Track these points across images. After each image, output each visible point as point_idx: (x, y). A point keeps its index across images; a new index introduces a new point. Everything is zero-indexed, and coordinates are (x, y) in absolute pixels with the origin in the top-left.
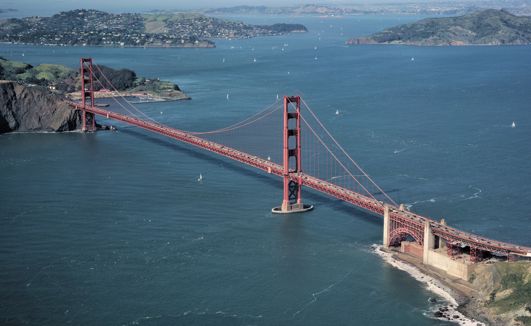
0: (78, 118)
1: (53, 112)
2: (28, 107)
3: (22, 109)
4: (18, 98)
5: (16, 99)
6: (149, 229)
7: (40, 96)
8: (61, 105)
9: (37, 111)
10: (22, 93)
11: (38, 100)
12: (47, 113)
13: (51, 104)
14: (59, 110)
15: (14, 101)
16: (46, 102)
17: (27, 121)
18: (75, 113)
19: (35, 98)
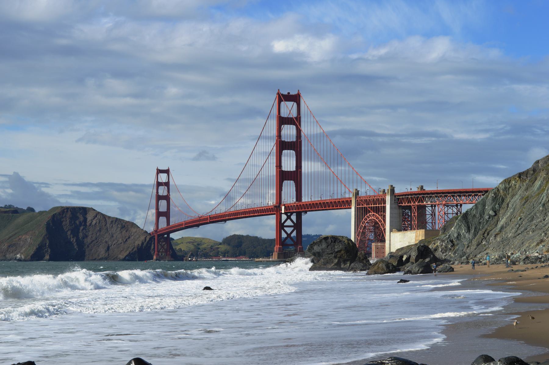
0: (153, 246)
1: (125, 240)
2: (98, 235)
3: (90, 237)
4: (88, 224)
7: (114, 222)
8: (136, 232)
9: (107, 239)
10: (94, 219)
11: (111, 226)
14: (132, 237)
15: (82, 228)
16: (119, 229)
17: (93, 251)
18: (149, 241)
19: (108, 225)
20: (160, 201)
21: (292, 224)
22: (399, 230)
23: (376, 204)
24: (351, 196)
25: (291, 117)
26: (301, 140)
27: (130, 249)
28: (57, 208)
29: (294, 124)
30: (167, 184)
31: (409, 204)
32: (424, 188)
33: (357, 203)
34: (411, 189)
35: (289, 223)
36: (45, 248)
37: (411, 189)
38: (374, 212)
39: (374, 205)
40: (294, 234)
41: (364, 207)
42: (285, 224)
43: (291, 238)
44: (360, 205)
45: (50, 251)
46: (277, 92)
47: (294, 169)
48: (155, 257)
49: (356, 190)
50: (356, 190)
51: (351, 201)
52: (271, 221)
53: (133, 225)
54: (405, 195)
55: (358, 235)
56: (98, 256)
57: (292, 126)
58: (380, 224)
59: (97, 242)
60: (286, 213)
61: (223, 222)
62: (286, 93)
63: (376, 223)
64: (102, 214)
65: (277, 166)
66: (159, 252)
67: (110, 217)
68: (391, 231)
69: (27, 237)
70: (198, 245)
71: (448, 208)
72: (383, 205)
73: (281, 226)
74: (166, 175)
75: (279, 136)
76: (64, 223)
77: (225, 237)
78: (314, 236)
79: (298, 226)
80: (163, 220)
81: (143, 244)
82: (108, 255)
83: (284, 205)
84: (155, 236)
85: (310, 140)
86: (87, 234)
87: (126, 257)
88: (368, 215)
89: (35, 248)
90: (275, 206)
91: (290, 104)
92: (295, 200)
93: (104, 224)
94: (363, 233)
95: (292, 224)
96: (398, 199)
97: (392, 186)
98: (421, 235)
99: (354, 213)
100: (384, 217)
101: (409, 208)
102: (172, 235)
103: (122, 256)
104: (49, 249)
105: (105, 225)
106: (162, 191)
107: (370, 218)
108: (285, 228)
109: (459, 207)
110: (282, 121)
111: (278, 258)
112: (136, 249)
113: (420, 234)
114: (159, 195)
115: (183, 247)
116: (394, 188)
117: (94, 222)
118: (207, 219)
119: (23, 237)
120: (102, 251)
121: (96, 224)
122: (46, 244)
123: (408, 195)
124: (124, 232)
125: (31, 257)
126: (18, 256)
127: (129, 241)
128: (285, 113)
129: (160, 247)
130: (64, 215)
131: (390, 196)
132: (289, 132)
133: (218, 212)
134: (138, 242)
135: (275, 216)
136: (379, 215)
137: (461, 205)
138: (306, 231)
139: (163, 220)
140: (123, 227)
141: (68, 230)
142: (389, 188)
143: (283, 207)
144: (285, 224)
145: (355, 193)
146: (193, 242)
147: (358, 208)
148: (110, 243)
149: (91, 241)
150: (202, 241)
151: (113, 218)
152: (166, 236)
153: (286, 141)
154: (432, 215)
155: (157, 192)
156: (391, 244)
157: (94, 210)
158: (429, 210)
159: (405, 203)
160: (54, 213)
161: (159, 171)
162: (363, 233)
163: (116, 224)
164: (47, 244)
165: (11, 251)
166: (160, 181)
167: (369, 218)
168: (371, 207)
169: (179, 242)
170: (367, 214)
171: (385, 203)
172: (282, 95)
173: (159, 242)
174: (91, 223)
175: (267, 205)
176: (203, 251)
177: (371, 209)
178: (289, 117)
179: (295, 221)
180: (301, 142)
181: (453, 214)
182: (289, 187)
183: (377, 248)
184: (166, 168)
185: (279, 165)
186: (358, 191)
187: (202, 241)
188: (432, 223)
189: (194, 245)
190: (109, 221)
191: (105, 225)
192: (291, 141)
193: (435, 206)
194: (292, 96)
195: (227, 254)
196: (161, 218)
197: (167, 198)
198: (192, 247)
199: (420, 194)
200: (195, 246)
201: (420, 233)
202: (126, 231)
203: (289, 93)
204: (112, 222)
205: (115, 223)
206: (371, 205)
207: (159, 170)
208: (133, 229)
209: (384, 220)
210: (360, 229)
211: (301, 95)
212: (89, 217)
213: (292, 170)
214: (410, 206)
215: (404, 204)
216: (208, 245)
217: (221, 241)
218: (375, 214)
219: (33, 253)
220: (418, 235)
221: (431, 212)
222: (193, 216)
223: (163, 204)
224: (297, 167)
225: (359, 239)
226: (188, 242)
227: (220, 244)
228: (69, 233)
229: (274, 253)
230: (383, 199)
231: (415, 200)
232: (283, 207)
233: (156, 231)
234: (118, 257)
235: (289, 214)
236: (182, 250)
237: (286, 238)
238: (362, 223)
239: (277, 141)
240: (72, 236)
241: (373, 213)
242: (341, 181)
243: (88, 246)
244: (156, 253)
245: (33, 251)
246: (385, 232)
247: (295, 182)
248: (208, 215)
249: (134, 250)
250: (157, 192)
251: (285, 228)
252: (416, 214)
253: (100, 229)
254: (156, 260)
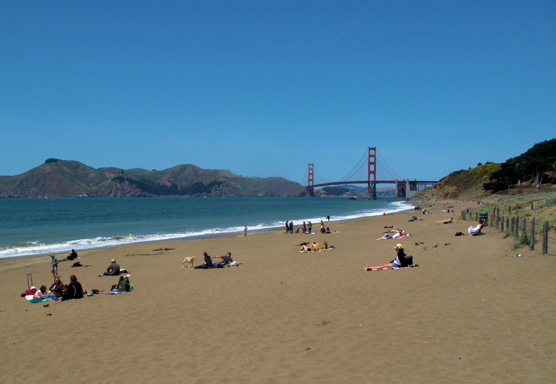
30: (312, 169)
73: (369, 187)
75: (369, 161)
79: (374, 187)
80: (311, 182)
91: (372, 150)
106: (311, 172)
152: (312, 188)
161: (309, 165)
185: (369, 169)
194: (373, 148)
196: (310, 182)
197: (312, 174)
224: (374, 170)
227: (321, 190)
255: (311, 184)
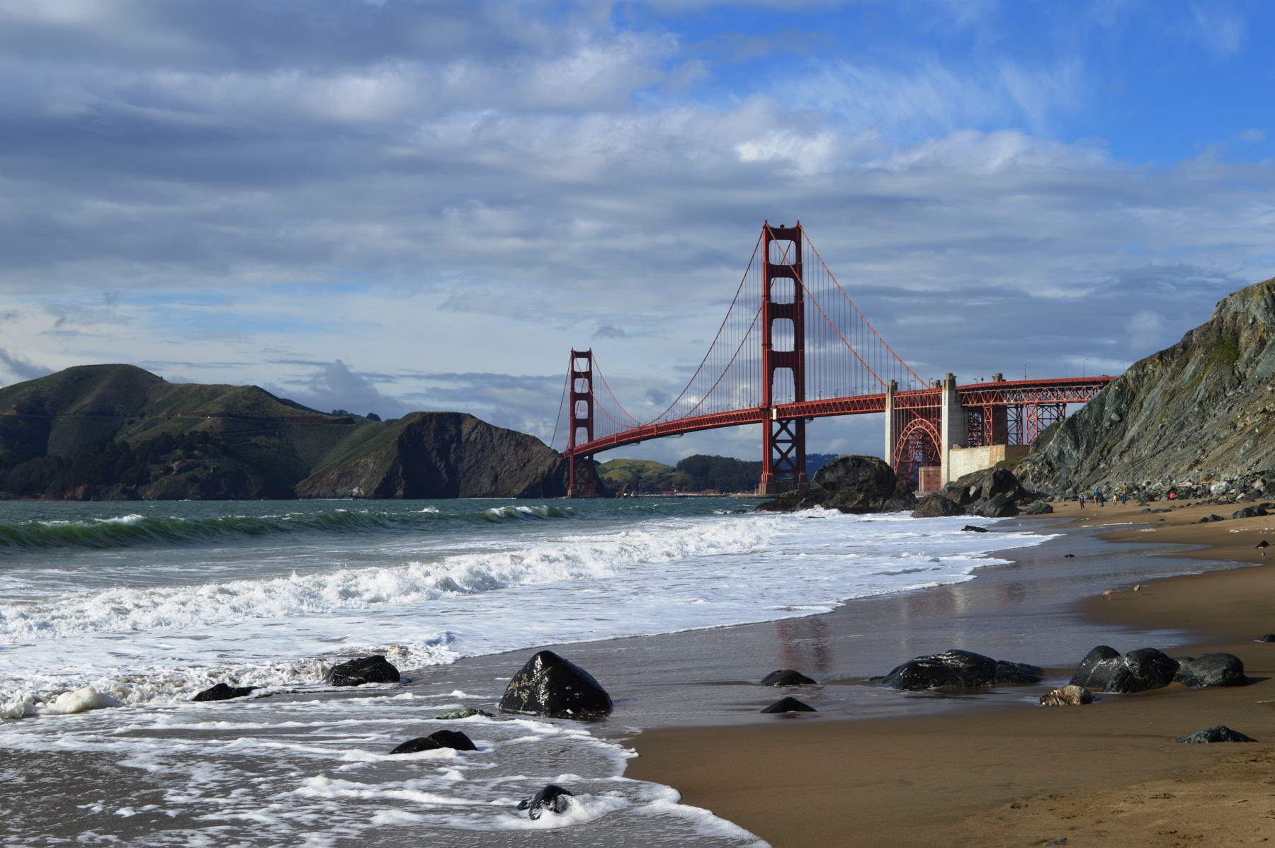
0: (566, 473)
1: (522, 465)
2: (479, 456)
3: (467, 459)
4: (463, 440)
5: (459, 441)
6: (677, 701)
7: (505, 436)
8: (539, 452)
9: (494, 464)
10: (473, 431)
11: (499, 443)
12: (511, 466)
13: (521, 451)
14: (534, 460)
15: (454, 446)
16: (513, 447)
17: (472, 481)
18: (561, 465)
19: (495, 441)
20: (577, 402)
21: (791, 439)
22: (964, 446)
23: (926, 405)
24: (885, 391)
25: (787, 264)
26: (803, 303)
27: (530, 480)
28: (415, 414)
29: (792, 276)
30: (588, 375)
31: (980, 404)
32: (1003, 378)
33: (895, 403)
34: (982, 380)
35: (784, 435)
36: (398, 478)
37: (982, 380)
38: (922, 417)
39: (922, 405)
40: (793, 454)
41: (907, 410)
42: (778, 438)
43: (789, 461)
44: (899, 406)
45: (404, 483)
46: (763, 225)
47: (792, 349)
48: (570, 492)
49: (893, 381)
50: (893, 381)
51: (884, 399)
52: (755, 431)
53: (535, 440)
54: (974, 389)
55: (896, 455)
56: (480, 490)
57: (787, 279)
58: (932, 437)
59: (478, 469)
60: (778, 420)
61: (677, 435)
62: (778, 226)
63: (926, 435)
64: (485, 423)
65: (764, 345)
66: (575, 482)
67: (498, 428)
68: (950, 447)
69: (369, 461)
70: (639, 471)
71: (1044, 410)
72: (936, 406)
73: (771, 441)
74: (585, 360)
75: (767, 295)
76: (425, 438)
77: (682, 459)
78: (825, 456)
79: (799, 440)
80: (582, 433)
81: (550, 470)
82: (496, 489)
83: (776, 407)
84: (569, 458)
85: (817, 302)
86: (462, 455)
87: (524, 492)
88: (913, 421)
89: (381, 478)
90: (762, 409)
91: (786, 242)
92: (794, 400)
93: (488, 439)
94: (905, 451)
95: (791, 439)
96: (961, 397)
97: (951, 375)
98: (998, 454)
99: (890, 418)
100: (939, 425)
101: (980, 410)
102: (596, 457)
103: (517, 491)
104: (403, 480)
105: (491, 442)
106: (581, 385)
107: (916, 427)
108: (778, 445)
109: (1061, 408)
110: (772, 271)
111: (767, 493)
112: (540, 478)
113: (997, 452)
114: (575, 393)
115: (615, 476)
116: (954, 378)
117: (473, 436)
118: (652, 430)
119: (362, 461)
120: (486, 482)
121: (476, 439)
122: (398, 471)
123: (978, 389)
124: (521, 451)
125: (376, 492)
126: (355, 490)
127: (529, 467)
128: (776, 259)
129: (577, 476)
130: (426, 426)
131: (949, 390)
132: (783, 290)
133: (670, 419)
134: (543, 468)
135: (762, 424)
136: (930, 422)
137: (1064, 405)
138: (810, 449)
139: (582, 433)
140: (519, 444)
141: (433, 449)
142: (946, 378)
143: (775, 411)
144: (778, 438)
145: (892, 386)
146: (630, 468)
147: (896, 410)
148: (498, 469)
149: (468, 466)
150: (644, 465)
151: (503, 429)
152: (587, 458)
153: (778, 303)
154: (1016, 421)
155: (573, 388)
156: (950, 468)
157: (473, 417)
158: (1011, 414)
159: (973, 403)
160: (411, 422)
161: (576, 355)
162: (905, 451)
163: (508, 439)
164: (400, 472)
165: (344, 483)
166: (576, 369)
167: (914, 427)
168: (918, 409)
169: (608, 467)
170: (911, 421)
171: (939, 402)
172: (772, 229)
173: (575, 467)
174: (469, 438)
175: (749, 408)
176: (646, 481)
177: (918, 413)
178: (783, 264)
179: (794, 433)
180: (802, 305)
181: (1051, 419)
182: (784, 377)
183: (927, 475)
184: (586, 350)
185: (768, 343)
186: (896, 384)
187: (644, 465)
188: (1017, 434)
189: (631, 472)
190: (496, 436)
191: (491, 442)
192: (786, 303)
193: (1022, 407)
194: (788, 230)
195: (684, 487)
197: (588, 397)
198: (629, 475)
199: (997, 388)
200: (634, 473)
201: (997, 450)
202: (524, 451)
203: (782, 226)
204: (501, 435)
205: (506, 438)
206: (918, 406)
207: (575, 352)
208: (534, 447)
209: (939, 431)
210: (900, 444)
211: (804, 229)
212: (466, 429)
213: (788, 350)
214: (981, 406)
215: (970, 404)
216: (654, 473)
217: (675, 466)
218: (924, 420)
219: (377, 485)
220: (994, 454)
221: (1015, 417)
222: (632, 425)
223: (582, 406)
224: (796, 345)
225: (898, 461)
226: (623, 468)
227: (674, 470)
228: (434, 453)
229: (760, 485)
230: (938, 396)
231: (990, 397)
232: (775, 411)
233: (571, 451)
234: (512, 492)
235: (784, 422)
236: (614, 480)
237: (779, 461)
238: (903, 435)
239: (764, 303)
240: (438, 459)
241: (920, 419)
242: (868, 368)
243: (464, 475)
244: (571, 485)
245: (379, 482)
246: (940, 450)
247: (793, 370)
248: (653, 424)
249: (537, 481)
250: (573, 388)
251: (778, 445)
252: (991, 420)
253: (483, 447)
254: (573, 496)
255: (582, 437)
